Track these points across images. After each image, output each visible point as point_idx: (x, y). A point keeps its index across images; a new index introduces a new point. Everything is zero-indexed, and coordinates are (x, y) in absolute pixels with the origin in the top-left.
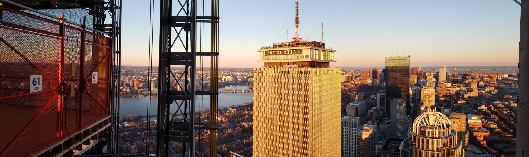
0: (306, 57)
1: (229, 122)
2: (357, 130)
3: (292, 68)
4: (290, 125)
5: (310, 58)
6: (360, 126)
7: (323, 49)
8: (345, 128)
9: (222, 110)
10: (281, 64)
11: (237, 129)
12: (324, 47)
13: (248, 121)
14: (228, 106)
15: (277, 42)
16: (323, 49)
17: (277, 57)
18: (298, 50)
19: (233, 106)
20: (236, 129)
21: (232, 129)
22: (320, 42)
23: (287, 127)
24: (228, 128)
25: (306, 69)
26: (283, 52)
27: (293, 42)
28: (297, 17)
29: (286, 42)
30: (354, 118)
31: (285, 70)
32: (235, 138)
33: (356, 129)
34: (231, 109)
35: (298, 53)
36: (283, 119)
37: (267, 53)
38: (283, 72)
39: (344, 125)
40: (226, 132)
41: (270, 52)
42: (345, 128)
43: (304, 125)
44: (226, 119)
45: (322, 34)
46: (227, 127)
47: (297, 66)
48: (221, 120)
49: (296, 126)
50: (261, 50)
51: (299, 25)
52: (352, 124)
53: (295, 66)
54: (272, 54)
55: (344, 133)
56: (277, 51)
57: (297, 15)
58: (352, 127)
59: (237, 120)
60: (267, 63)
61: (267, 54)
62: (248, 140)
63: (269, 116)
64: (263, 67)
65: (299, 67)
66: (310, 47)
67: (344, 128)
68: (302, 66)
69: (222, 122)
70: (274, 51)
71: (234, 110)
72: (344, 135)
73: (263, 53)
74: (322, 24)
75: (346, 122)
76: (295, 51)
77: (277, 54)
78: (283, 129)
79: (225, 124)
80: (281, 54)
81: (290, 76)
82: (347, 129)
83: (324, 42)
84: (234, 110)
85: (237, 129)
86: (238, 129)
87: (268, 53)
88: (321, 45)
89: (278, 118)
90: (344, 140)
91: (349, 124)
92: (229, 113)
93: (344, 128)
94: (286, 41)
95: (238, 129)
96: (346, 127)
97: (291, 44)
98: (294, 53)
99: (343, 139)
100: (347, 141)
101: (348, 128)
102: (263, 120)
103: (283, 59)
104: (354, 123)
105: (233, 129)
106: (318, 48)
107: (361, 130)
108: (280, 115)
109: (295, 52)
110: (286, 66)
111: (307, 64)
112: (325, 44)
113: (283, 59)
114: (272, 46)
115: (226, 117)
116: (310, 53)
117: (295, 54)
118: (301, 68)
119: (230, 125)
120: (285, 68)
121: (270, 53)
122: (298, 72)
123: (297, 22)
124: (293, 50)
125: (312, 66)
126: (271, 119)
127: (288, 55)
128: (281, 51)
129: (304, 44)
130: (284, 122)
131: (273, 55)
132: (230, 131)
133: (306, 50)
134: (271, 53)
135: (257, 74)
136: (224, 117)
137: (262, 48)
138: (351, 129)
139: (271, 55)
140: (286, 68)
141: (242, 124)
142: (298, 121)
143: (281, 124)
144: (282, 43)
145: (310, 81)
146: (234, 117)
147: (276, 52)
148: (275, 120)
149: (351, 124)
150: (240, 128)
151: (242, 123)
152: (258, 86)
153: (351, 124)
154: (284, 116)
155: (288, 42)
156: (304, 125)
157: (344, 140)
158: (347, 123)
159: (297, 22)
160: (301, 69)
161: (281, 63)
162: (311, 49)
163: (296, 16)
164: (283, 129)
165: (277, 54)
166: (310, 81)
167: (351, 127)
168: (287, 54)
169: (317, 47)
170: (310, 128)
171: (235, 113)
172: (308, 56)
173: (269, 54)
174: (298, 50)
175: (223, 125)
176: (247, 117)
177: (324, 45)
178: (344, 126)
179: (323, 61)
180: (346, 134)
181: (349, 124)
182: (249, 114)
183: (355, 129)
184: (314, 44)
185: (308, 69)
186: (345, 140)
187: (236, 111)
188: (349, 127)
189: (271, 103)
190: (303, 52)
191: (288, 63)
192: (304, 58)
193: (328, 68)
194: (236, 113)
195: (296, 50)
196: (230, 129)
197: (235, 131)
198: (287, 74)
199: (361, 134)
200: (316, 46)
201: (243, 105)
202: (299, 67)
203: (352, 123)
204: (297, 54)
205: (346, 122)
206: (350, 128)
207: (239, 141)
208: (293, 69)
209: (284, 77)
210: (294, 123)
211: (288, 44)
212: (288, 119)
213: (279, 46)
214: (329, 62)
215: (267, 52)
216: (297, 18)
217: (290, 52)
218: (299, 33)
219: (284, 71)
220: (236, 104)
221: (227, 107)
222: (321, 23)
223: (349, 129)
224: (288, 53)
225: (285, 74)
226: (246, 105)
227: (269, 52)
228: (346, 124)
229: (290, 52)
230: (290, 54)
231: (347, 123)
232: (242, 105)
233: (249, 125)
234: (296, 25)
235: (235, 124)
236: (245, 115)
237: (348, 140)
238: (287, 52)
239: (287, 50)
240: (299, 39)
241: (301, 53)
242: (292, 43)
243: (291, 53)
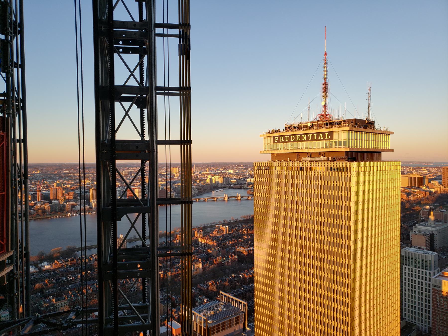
0: (340, 144)
1: (218, 245)
2: (432, 274)
3: (316, 161)
4: (314, 254)
5: (347, 146)
6: (439, 268)
7: (371, 131)
8: (409, 269)
9: (208, 227)
10: (298, 156)
11: (230, 256)
12: (374, 127)
13: (247, 245)
14: (217, 222)
15: (290, 122)
16: (371, 131)
17: (291, 145)
18: (327, 134)
19: (224, 221)
20: (229, 257)
21: (223, 257)
22: (365, 119)
23: (308, 257)
24: (217, 255)
25: (340, 164)
26: (301, 138)
27: (318, 121)
28: (326, 83)
29: (307, 122)
30: (427, 253)
31: (304, 166)
32: (227, 270)
33: (430, 273)
34: (221, 226)
35: (327, 138)
36: (301, 242)
37: (276, 140)
38: (302, 169)
39: (406, 262)
40: (213, 262)
41: (281, 137)
42: (409, 269)
43: (337, 255)
44: (213, 241)
45: (369, 106)
46: (215, 254)
47: (325, 158)
48: (207, 244)
49: (322, 255)
50: (265, 135)
51: (328, 94)
52: (422, 263)
53: (322, 158)
54: (283, 141)
55: (405, 275)
56: (292, 136)
57: (325, 79)
58: (422, 269)
59: (230, 243)
60: (275, 154)
61: (276, 141)
62: (247, 274)
63: (280, 237)
64: (270, 161)
65: (328, 160)
66: (348, 128)
67: (405, 268)
68: (334, 159)
69: (208, 246)
70: (286, 137)
71: (226, 228)
72: (405, 279)
73: (269, 139)
74: (370, 90)
75: (409, 258)
76: (321, 134)
77: (292, 140)
78: (301, 259)
79: (213, 249)
81: (313, 175)
82: (412, 269)
83: (372, 119)
84: (226, 228)
85: (230, 256)
86: (232, 256)
87: (277, 139)
88: (367, 123)
89: (294, 240)
90: (405, 289)
91: (415, 262)
92: (218, 232)
93: (405, 268)
94: (307, 121)
95: (232, 256)
96: (409, 265)
97: (315, 124)
98: (319, 139)
99: (404, 287)
100: (412, 290)
101: (414, 269)
102: (270, 243)
103: (300, 148)
104: (426, 261)
105: (225, 257)
106: (362, 130)
107: (440, 275)
108: (296, 236)
109: (322, 137)
110: (307, 158)
111: (343, 155)
112: (374, 122)
113: (300, 148)
114: (282, 128)
115: (214, 238)
116: (347, 138)
117: (321, 140)
118: (332, 163)
119: (219, 251)
120: (303, 162)
121: (281, 139)
122: (327, 169)
123: (325, 90)
124: (318, 134)
125: (350, 158)
126: (284, 242)
127: (310, 142)
128: (297, 136)
129: (338, 123)
130: (303, 247)
131: (285, 142)
132: (220, 259)
133: (341, 134)
134: (282, 139)
135: (260, 172)
136: (210, 239)
137: (268, 131)
138: (419, 271)
139: (282, 142)
140: (306, 161)
141: (238, 249)
142: (326, 248)
143: (298, 250)
144: (300, 123)
145: (348, 183)
146: (226, 238)
147: (290, 138)
148: (289, 243)
149: (419, 263)
150: (235, 255)
151: (238, 247)
152: (262, 191)
153: (419, 263)
154: (304, 238)
155: (310, 121)
156: (337, 255)
157: (405, 289)
158: (412, 259)
159: (325, 90)
160: (331, 164)
161: (298, 154)
162: (349, 131)
163: (323, 81)
164: (301, 259)
165: (292, 140)
166: (348, 183)
167: (419, 268)
168: (308, 140)
169: (360, 128)
170: (347, 260)
171: (227, 233)
172: (345, 142)
173: (278, 141)
174: (327, 134)
175: (209, 251)
176: (246, 237)
177: (374, 124)
178: (406, 265)
179: (372, 151)
180: (409, 279)
181: (415, 262)
182: (249, 234)
183: (428, 272)
184: (354, 122)
185: (344, 163)
186: (407, 288)
187: (229, 228)
188: (415, 267)
189: (283, 217)
190: (336, 136)
191: (310, 154)
192: (336, 145)
193: (378, 163)
194: (229, 231)
195: (323, 134)
196: (220, 257)
197: (227, 260)
198: (308, 172)
199: (441, 282)
200: (358, 127)
201: (239, 219)
202: (328, 160)
203: (422, 261)
204: (324, 139)
205: (409, 258)
206: (417, 269)
207: (233, 275)
208: (317, 163)
209: (303, 177)
210: (320, 251)
211: (309, 124)
212: (309, 244)
213: (295, 127)
214: (380, 152)
215: (276, 138)
216: (325, 84)
217: (313, 138)
218: (328, 107)
219: (303, 167)
220: (228, 220)
221: (214, 223)
222: (368, 87)
223: (415, 270)
224: (310, 139)
225: (305, 172)
226: (243, 219)
227: (279, 139)
228: (409, 261)
229: (313, 138)
230: (313, 140)
231: (412, 259)
232: (237, 219)
233: (248, 250)
234: (324, 94)
235: (228, 249)
236: (243, 235)
237: (413, 289)
238: (307, 138)
239: (307, 134)
240: (329, 117)
241: (332, 138)
242: (316, 123)
243: (315, 139)
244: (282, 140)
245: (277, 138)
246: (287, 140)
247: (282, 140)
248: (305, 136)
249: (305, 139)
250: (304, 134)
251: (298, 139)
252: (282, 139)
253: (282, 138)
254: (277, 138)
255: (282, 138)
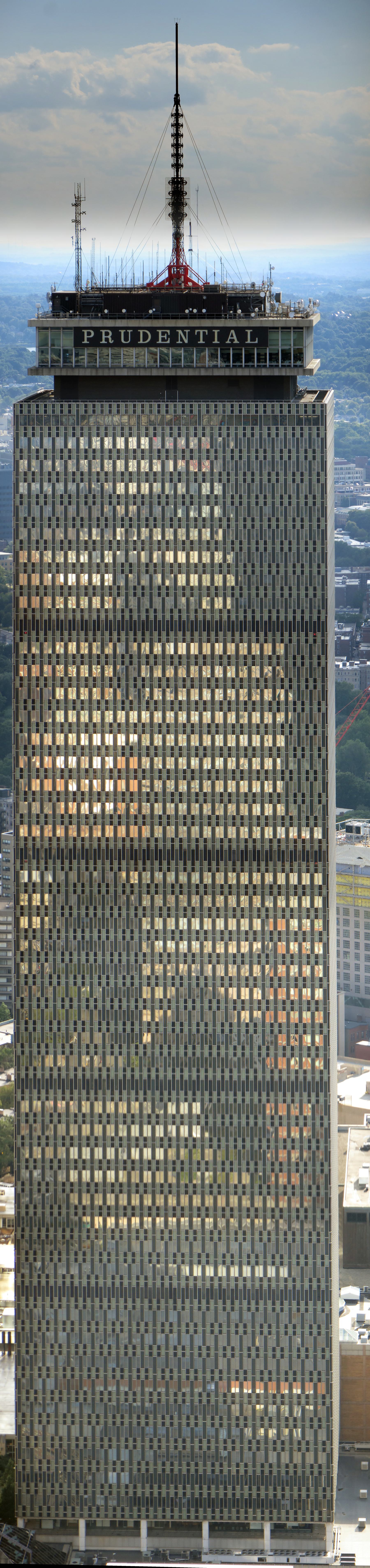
37: (86, 337)
54: (111, 341)
56: (141, 332)
61: (86, 342)
77: (141, 342)
80: (160, 342)
121: (104, 337)
128: (160, 332)
139: (108, 345)
165: (141, 342)
239: (193, 329)
244: (107, 340)
245: (89, 334)
246: (126, 339)
247: (107, 340)
248: (185, 334)
249: (186, 341)
250: (182, 329)
251: (163, 339)
252: (109, 337)
253: (107, 334)
254: (89, 334)
255: (107, 334)
